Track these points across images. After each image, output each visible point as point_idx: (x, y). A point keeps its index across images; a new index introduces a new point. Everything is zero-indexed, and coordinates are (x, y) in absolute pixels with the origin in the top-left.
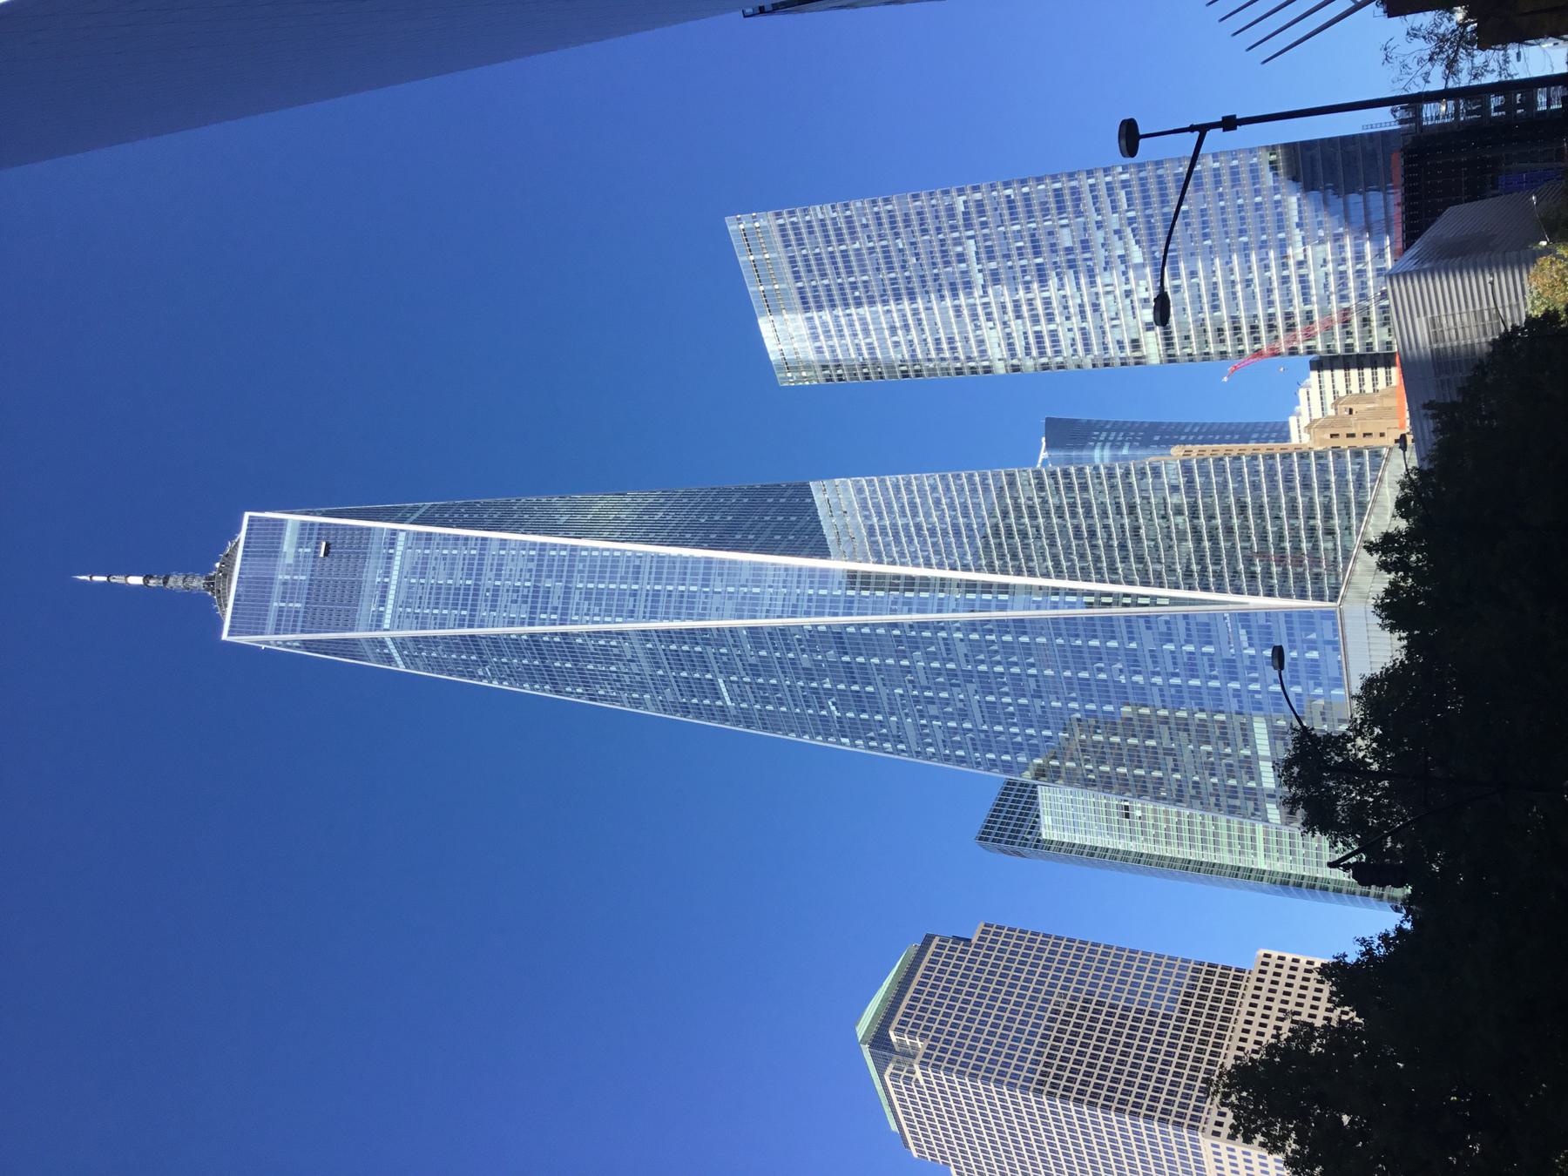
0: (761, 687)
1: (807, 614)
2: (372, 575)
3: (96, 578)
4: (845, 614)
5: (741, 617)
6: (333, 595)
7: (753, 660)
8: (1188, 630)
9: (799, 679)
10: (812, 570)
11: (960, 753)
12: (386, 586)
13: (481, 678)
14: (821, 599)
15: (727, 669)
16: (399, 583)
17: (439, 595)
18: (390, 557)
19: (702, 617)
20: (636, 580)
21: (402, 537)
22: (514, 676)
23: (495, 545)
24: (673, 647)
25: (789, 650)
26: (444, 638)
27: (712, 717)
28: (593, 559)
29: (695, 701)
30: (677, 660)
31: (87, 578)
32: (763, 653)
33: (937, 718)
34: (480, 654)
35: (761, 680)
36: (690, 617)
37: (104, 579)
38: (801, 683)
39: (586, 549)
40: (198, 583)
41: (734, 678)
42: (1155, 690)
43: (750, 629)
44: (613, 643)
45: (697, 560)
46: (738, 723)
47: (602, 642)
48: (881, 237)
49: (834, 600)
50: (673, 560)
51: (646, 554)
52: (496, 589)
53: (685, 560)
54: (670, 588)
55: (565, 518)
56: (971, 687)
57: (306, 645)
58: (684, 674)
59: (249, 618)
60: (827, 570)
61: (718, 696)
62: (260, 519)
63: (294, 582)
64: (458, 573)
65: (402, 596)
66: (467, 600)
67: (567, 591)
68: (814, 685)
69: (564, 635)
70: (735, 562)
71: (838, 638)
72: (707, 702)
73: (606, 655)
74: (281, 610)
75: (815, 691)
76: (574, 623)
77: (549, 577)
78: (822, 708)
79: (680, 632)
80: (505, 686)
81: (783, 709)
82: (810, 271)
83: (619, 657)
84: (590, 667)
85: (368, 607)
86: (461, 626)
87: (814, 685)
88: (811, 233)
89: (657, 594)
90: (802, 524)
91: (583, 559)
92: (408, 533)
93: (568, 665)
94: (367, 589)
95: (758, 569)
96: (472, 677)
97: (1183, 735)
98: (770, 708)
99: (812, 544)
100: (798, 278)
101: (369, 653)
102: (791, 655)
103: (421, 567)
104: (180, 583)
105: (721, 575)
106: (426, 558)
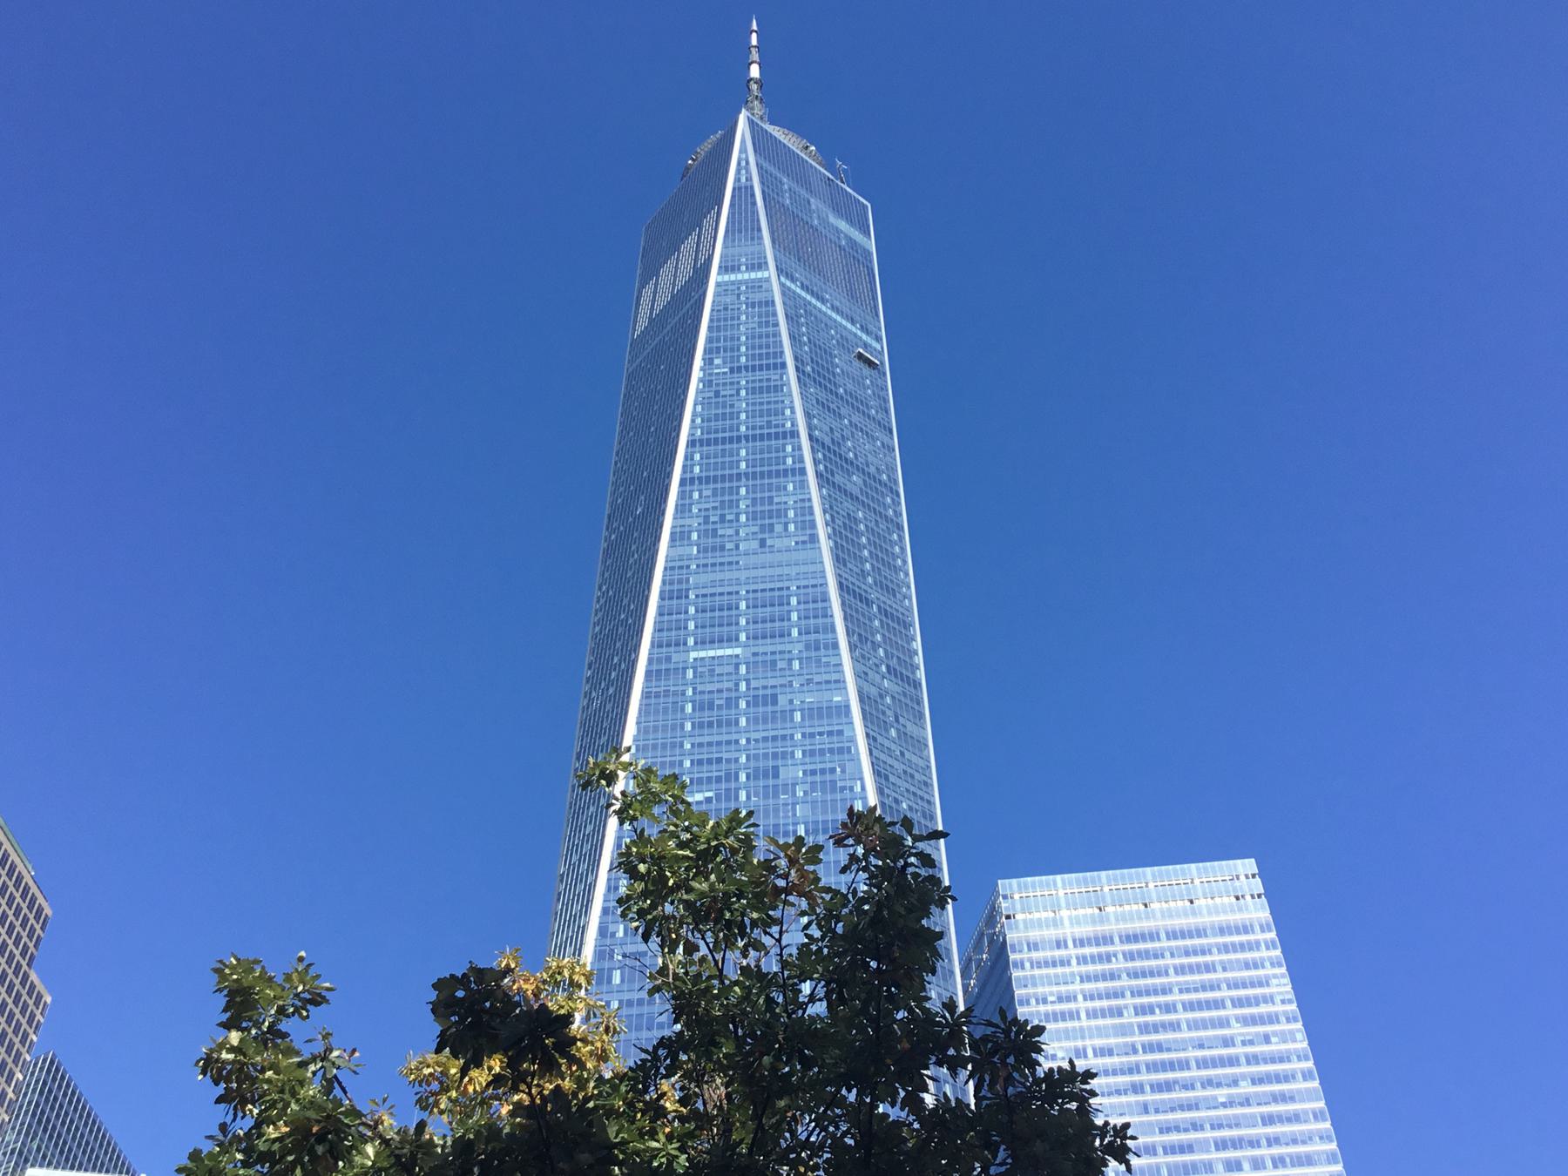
0: (731, 703)
3: (754, 36)
5: (861, 700)
7: (782, 700)
12: (823, 301)
13: (708, 361)
18: (853, 322)
19: (852, 647)
23: (886, 440)
26: (777, 334)
28: (893, 544)
31: (755, 27)
41: (743, 669)
48: (1253, 1059)
61: (701, 643)
73: (767, 518)
76: (820, 487)
79: (826, 614)
81: (688, 726)
82: (1187, 954)
84: (743, 491)
86: (796, 359)
88: (1247, 966)
100: (1172, 935)
102: (798, 754)
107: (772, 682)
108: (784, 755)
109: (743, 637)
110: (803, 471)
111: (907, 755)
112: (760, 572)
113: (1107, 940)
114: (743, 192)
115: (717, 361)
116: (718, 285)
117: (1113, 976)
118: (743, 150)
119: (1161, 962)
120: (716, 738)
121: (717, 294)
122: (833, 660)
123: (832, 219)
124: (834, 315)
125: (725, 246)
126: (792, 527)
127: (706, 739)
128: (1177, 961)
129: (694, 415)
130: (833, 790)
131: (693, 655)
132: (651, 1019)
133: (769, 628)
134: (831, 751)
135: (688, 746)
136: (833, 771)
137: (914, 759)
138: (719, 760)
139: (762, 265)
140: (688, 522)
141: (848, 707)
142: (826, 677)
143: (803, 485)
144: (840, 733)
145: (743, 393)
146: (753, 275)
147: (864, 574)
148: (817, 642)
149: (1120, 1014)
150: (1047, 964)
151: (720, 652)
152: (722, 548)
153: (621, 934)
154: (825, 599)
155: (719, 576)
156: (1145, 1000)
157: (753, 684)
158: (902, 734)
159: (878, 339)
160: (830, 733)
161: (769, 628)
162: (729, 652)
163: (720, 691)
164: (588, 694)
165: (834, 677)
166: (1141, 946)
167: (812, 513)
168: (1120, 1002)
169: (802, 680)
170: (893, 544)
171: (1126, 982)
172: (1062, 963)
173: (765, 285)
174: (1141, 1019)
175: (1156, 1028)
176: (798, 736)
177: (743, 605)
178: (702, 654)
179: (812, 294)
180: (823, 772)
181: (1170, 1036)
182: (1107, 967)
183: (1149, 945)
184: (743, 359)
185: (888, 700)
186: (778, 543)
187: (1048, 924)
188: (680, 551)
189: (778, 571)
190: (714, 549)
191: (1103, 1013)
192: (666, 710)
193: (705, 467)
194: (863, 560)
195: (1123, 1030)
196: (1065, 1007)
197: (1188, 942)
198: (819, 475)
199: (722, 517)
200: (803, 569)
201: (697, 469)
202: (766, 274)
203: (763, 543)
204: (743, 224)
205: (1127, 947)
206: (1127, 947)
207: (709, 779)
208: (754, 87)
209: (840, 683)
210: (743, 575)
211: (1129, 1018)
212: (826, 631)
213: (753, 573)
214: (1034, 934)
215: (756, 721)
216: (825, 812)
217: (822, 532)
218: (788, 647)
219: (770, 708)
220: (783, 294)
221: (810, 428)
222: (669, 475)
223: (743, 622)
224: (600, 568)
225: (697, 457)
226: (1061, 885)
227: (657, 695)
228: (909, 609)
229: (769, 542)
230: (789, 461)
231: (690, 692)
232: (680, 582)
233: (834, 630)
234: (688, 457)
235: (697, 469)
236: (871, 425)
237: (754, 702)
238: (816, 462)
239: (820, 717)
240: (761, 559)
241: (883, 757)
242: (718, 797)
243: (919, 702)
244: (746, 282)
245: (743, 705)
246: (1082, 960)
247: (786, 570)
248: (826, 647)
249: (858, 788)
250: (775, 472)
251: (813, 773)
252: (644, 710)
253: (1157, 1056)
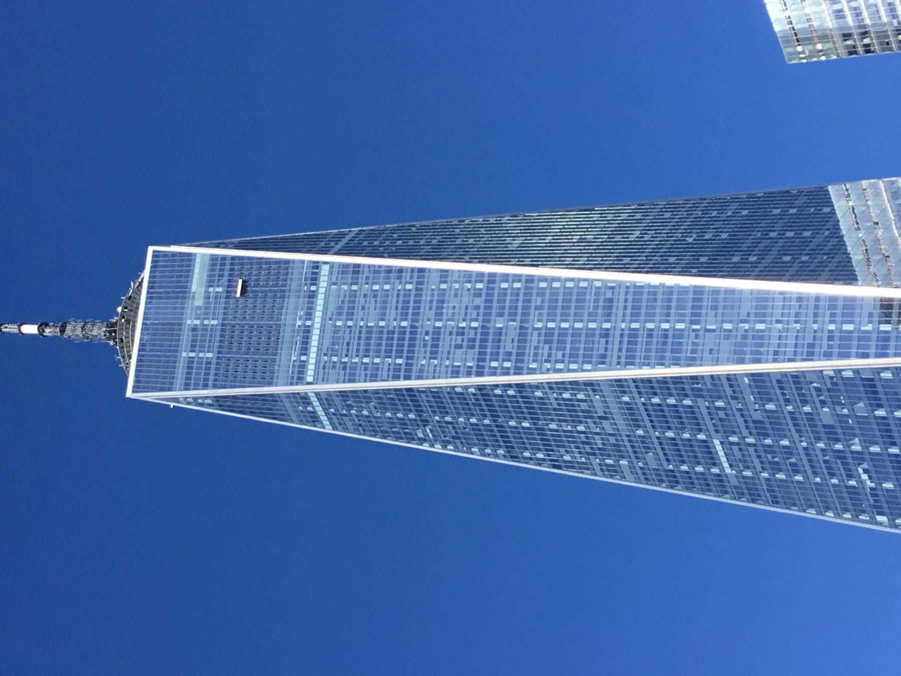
0: (768, 449)
1: (828, 356)
2: (292, 317)
4: (878, 356)
5: (741, 361)
6: (250, 343)
7: (758, 416)
9: (819, 439)
10: (834, 299)
12: (308, 331)
13: (421, 441)
14: (846, 337)
15: (725, 428)
16: (323, 326)
17: (369, 340)
18: (312, 296)
20: (608, 317)
21: (325, 269)
22: (458, 438)
23: (435, 278)
24: (656, 400)
25: (805, 402)
26: (376, 392)
27: (707, 488)
28: (554, 292)
29: (684, 468)
30: (661, 417)
32: (770, 406)
34: (419, 412)
35: (768, 441)
36: (676, 362)
38: (821, 445)
39: (545, 279)
40: (98, 331)
43: (753, 376)
44: (581, 396)
45: (683, 290)
46: (740, 496)
47: (566, 395)
49: (864, 337)
50: (653, 291)
51: (620, 284)
52: (437, 332)
53: (669, 291)
54: (650, 326)
55: (518, 241)
57: (219, 401)
58: (670, 434)
59: (156, 372)
60: (854, 299)
62: (165, 254)
63: (205, 328)
64: (392, 313)
65: (327, 343)
66: (403, 345)
67: (523, 333)
68: (838, 446)
69: (520, 387)
70: (733, 292)
71: (869, 386)
72: (699, 469)
73: (571, 411)
74: (191, 361)
75: (840, 455)
76: (532, 371)
77: (501, 315)
78: (850, 476)
79: (664, 381)
80: (450, 451)
81: (799, 478)
83: (588, 414)
84: (553, 426)
85: (289, 356)
86: (396, 377)
87: (838, 446)
89: (633, 334)
90: (819, 240)
91: (541, 293)
92: (332, 265)
93: (526, 424)
94: (286, 334)
95: (762, 299)
96: (410, 438)
98: (781, 476)
99: (832, 266)
101: (291, 411)
102: (807, 409)
103: (347, 307)
104: (79, 332)
105: (714, 308)
106: (353, 295)
110: (518, 385)
115: (420, 435)
121: (346, 429)
122: (708, 382)
125: (292, 421)
131: (728, 471)
136: (817, 389)
141: (752, 375)
144: (778, 381)
151: (721, 454)
162: (719, 448)
169: (733, 402)
173: (324, 397)
176: (790, 408)
178: (726, 465)
198: (518, 371)
201: (540, 455)
209: (731, 379)
218: (705, 412)
225: (527, 454)
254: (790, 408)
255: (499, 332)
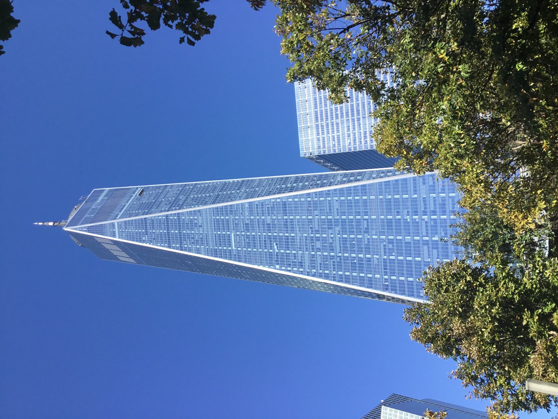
0: (248, 237)
1: (274, 194)
7: (247, 222)
8: (443, 186)
11: (327, 272)
12: (125, 205)
13: (144, 241)
14: (281, 188)
18: (132, 196)
19: (232, 200)
23: (169, 187)
26: (135, 220)
28: (201, 187)
33: (319, 250)
37: (42, 224)
41: (238, 233)
42: (424, 223)
56: (338, 228)
61: (230, 245)
73: (192, 225)
76: (183, 208)
79: (222, 208)
81: (255, 250)
82: (321, 103)
84: (184, 232)
86: (143, 215)
97: (435, 251)
98: (249, 249)
100: (316, 107)
102: (263, 217)
107: (242, 225)
108: (263, 222)
109: (228, 233)
110: (178, 214)
111: (264, 185)
112: (209, 227)
113: (317, 126)
114: (89, 229)
115: (144, 239)
116: (119, 238)
117: (327, 125)
118: (76, 229)
119: (324, 111)
120: (258, 242)
121: (122, 238)
122: (236, 206)
123: (99, 201)
124: (130, 202)
125: (107, 235)
126: (196, 218)
127: (259, 244)
128: (323, 106)
129: (161, 246)
130: (274, 208)
131: (234, 248)
132: (338, 262)
133: (226, 225)
134: (262, 208)
135: (261, 250)
136: (268, 208)
137: (265, 183)
138: (265, 241)
139: (113, 225)
140: (194, 249)
141: (249, 203)
142: (241, 209)
143: (183, 214)
144: (257, 205)
145: (154, 231)
146: (116, 227)
147: (210, 196)
148: (230, 211)
149: (338, 123)
150: (324, 144)
151: (233, 240)
152: (202, 238)
153: (315, 271)
154: (217, 208)
155: (210, 240)
156: (334, 116)
157: (242, 230)
158: (258, 186)
159: (137, 188)
160: (257, 208)
161: (226, 225)
162: (233, 237)
163: (244, 240)
164: (245, 279)
165: (240, 206)
166: (319, 116)
167: (191, 211)
168: (335, 123)
169: (241, 216)
170: (201, 187)
171: (329, 121)
172: (324, 139)
174: (339, 117)
175: (342, 114)
176: (258, 217)
177: (219, 233)
178: (233, 245)
179: (122, 209)
180: (268, 210)
181: (344, 109)
182: (325, 127)
183: (319, 114)
184: (143, 231)
185: (247, 190)
186: (200, 222)
187: (313, 143)
188: (202, 251)
189: (209, 222)
190: (202, 241)
191: (338, 128)
192: (250, 256)
193: (177, 243)
194: (206, 196)
195: (342, 122)
196: (336, 139)
197: (318, 103)
198: (180, 209)
199: (192, 238)
200: (208, 215)
201: (178, 245)
202: (116, 223)
203: (200, 226)
204: (100, 230)
205: (319, 120)
206: (319, 120)
207: (271, 244)
208: (56, 224)
209: (242, 204)
210: (210, 233)
211: (339, 121)
212: (227, 208)
213: (209, 229)
214: (316, 146)
215: (253, 230)
216: (280, 210)
217: (197, 208)
218: (232, 220)
219: (250, 226)
220: (122, 218)
221: (165, 211)
222: (179, 254)
223: (224, 233)
224: (208, 274)
225: (174, 245)
226: (302, 138)
227: (245, 259)
228: (221, 182)
229: (200, 224)
230: (175, 218)
231: (245, 249)
232: (212, 251)
233: (227, 206)
234: (174, 248)
235: (178, 245)
236: (164, 192)
237: (248, 230)
238: (176, 210)
239: (252, 211)
240: (205, 227)
241: (264, 193)
242: (275, 241)
243: (248, 181)
244: (118, 229)
245: (248, 234)
246: (323, 133)
247: (209, 220)
248: (232, 208)
249: (273, 200)
250: (179, 222)
251: (269, 213)
252: (250, 263)
253: (350, 113)
254: (258, 217)
255: (179, 199)
